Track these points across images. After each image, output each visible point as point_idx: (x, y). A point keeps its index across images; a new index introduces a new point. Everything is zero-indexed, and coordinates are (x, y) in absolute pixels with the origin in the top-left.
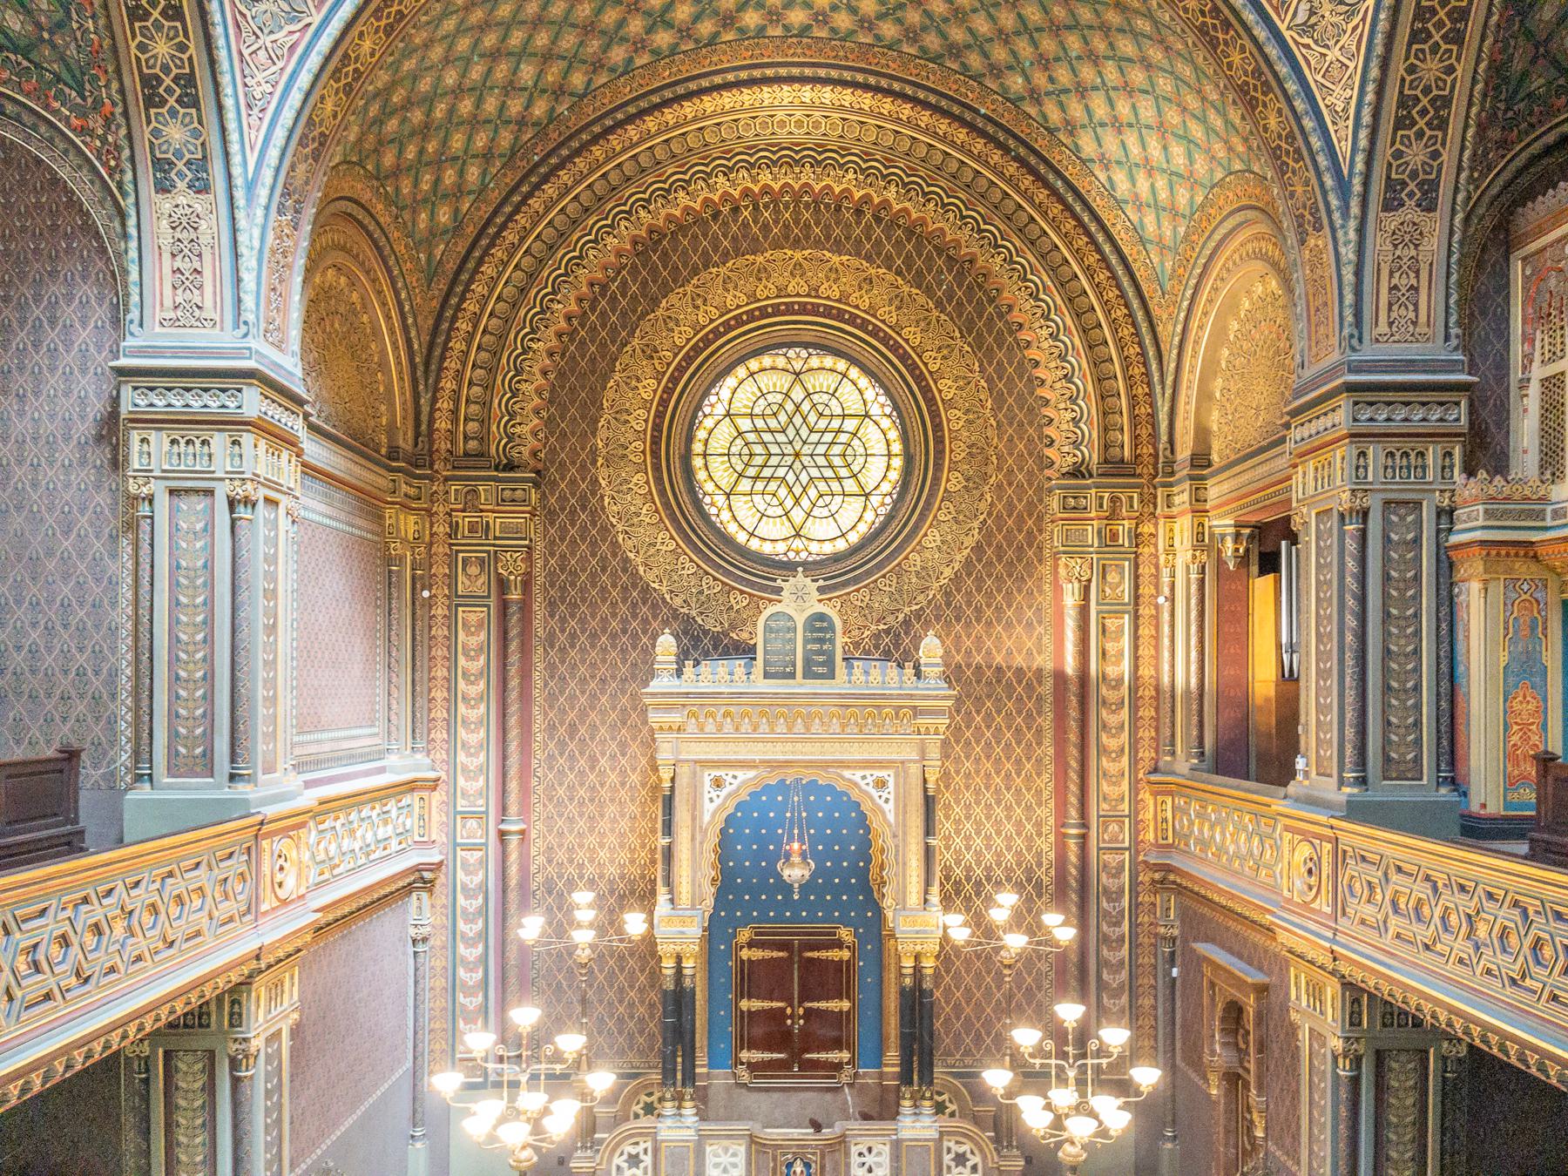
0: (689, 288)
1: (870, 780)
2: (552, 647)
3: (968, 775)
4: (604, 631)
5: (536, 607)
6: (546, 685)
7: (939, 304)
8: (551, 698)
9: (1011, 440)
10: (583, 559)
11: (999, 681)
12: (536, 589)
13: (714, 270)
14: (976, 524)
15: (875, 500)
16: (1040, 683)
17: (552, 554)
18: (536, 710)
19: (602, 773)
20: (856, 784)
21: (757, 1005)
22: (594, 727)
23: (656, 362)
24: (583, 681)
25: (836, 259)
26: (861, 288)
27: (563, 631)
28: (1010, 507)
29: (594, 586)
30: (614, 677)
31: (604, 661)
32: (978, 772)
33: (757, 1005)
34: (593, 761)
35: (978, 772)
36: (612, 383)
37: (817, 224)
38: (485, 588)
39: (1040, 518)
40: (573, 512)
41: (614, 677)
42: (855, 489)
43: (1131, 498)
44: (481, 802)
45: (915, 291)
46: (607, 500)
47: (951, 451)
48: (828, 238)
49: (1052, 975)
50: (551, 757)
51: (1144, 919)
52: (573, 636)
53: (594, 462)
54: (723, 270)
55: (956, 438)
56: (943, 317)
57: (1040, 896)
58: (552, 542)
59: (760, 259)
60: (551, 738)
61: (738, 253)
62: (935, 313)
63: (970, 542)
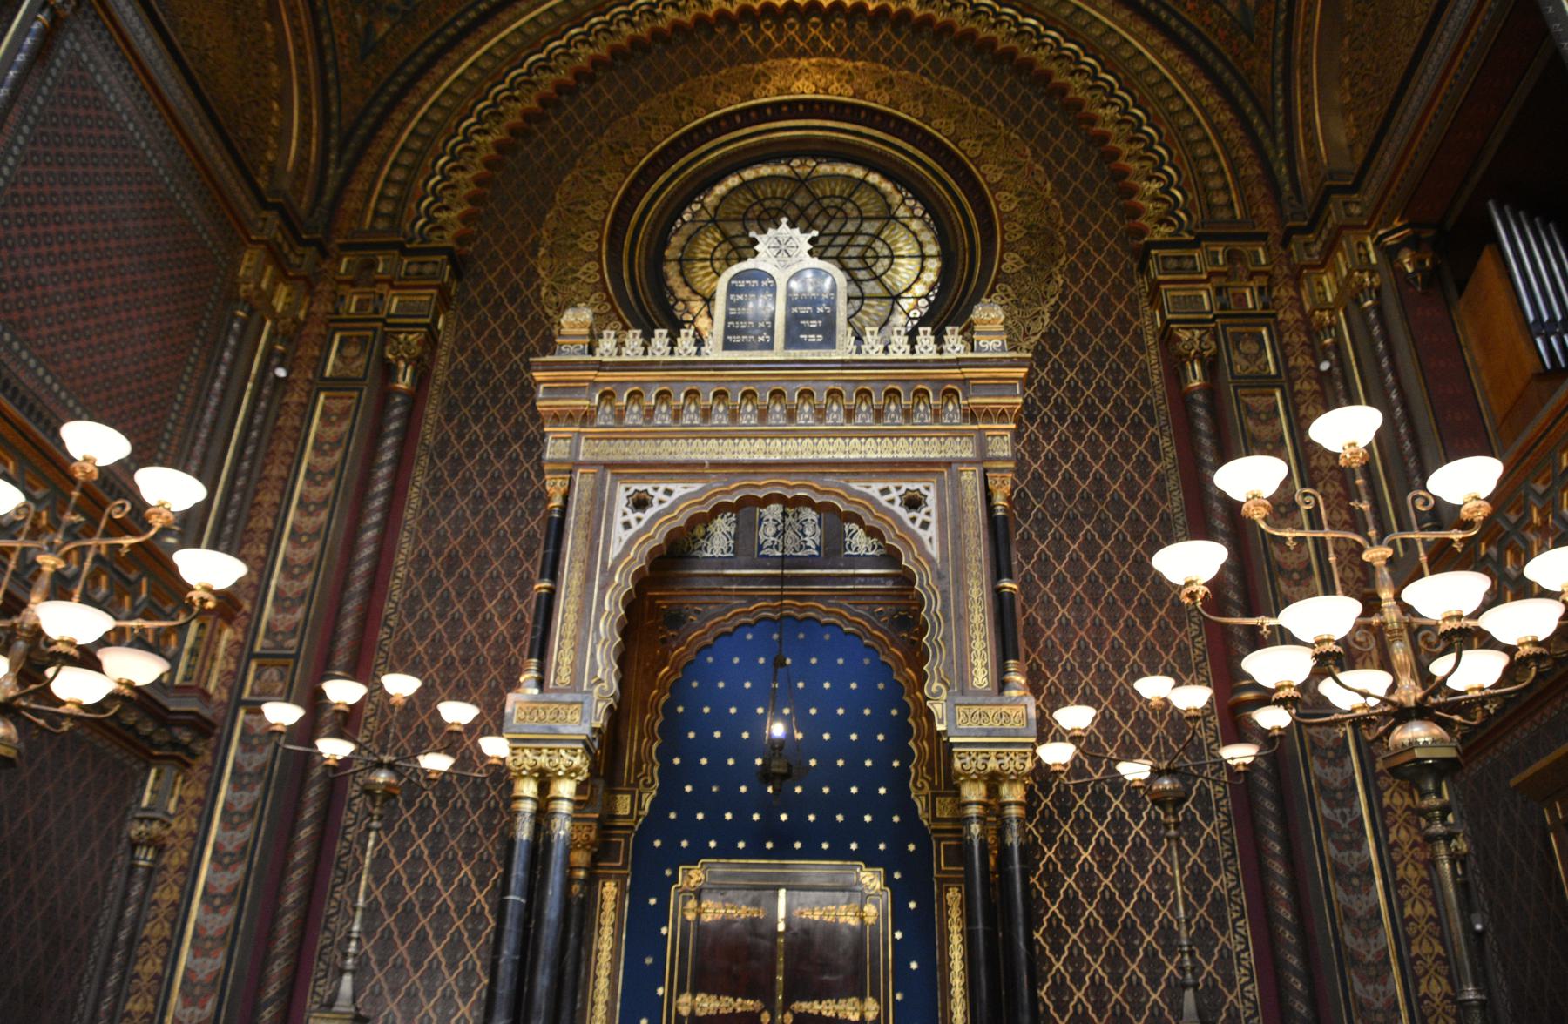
0: (672, 94)
1: (894, 494)
2: (442, 456)
3: (1064, 627)
4: (517, 437)
5: (429, 410)
6: (425, 503)
7: (976, 100)
8: (428, 521)
9: (1081, 221)
10: (504, 355)
11: (1101, 496)
12: (433, 389)
13: (704, 78)
14: (1046, 308)
15: (906, 303)
16: (1164, 499)
17: (462, 350)
18: (404, 537)
19: (488, 623)
20: (871, 499)
21: (708, 1004)
22: (483, 561)
23: (626, 157)
24: (479, 500)
25: (849, 65)
26: (878, 86)
27: (460, 437)
28: (1090, 291)
29: (512, 383)
30: (522, 494)
31: (512, 474)
32: (1080, 622)
33: (708, 1004)
34: (475, 606)
35: (1080, 622)
36: (569, 177)
37: (827, 38)
38: (361, 371)
39: (1133, 303)
40: (499, 304)
41: (522, 494)
42: (879, 291)
43: (1256, 253)
44: (293, 642)
45: (944, 88)
46: (544, 291)
47: (1003, 232)
48: (839, 49)
49: (1249, 957)
50: (414, 600)
51: (1400, 835)
52: (474, 444)
53: (534, 254)
54: (713, 78)
55: (1009, 219)
56: (981, 110)
57: (1208, 817)
58: (466, 337)
59: (760, 67)
60: (419, 573)
61: (731, 63)
62: (971, 106)
63: (1040, 328)
